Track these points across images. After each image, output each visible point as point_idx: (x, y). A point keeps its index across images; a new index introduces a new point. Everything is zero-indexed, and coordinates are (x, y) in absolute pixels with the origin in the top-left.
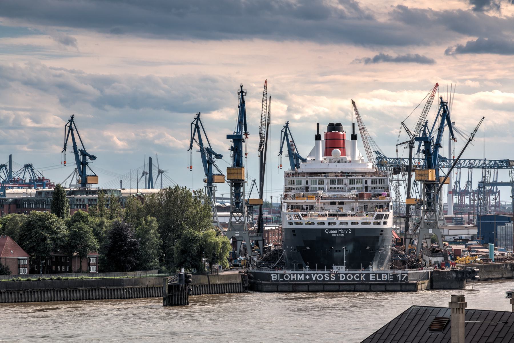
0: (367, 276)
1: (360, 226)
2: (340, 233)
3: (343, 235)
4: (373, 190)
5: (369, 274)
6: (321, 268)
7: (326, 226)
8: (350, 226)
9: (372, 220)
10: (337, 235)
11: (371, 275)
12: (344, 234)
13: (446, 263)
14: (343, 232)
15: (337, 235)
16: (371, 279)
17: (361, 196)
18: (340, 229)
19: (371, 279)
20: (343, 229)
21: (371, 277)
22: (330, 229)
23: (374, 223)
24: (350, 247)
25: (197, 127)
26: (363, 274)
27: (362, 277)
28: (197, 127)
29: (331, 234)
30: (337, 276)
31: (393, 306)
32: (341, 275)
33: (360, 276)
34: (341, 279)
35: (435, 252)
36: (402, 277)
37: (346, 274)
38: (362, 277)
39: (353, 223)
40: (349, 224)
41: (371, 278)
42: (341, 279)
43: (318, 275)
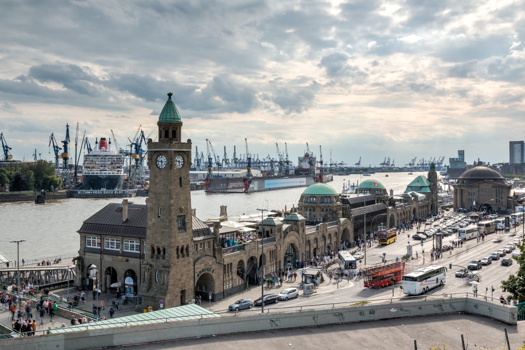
0: (114, 192)
1: (111, 174)
4: (116, 161)
6: (97, 189)
7: (99, 174)
8: (107, 174)
9: (116, 172)
13: (142, 187)
17: (112, 164)
24: (108, 182)
25: (52, 138)
28: (52, 138)
30: (103, 192)
31: (103, 203)
35: (138, 183)
41: (115, 192)
43: (96, 192)
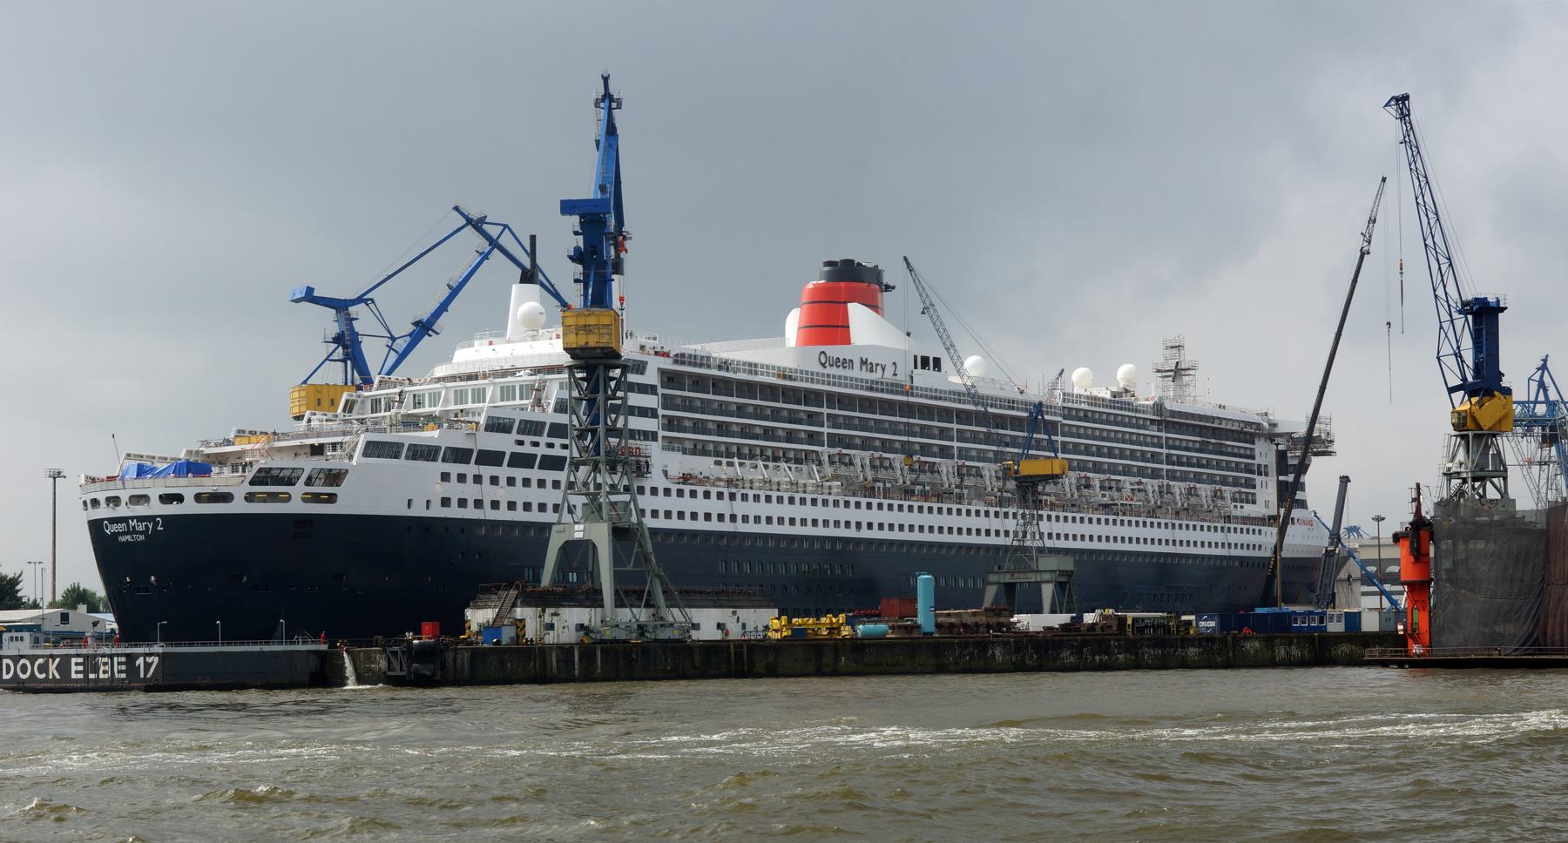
1: (190, 507)
2: (135, 532)
3: (142, 538)
5: (67, 658)
8: (156, 508)
10: (128, 538)
11: (74, 660)
12: (145, 533)
14: (141, 527)
15: (128, 538)
16: (74, 676)
18: (132, 518)
19: (74, 676)
20: (141, 519)
21: (74, 668)
22: (113, 521)
23: (250, 498)
26: (53, 657)
27: (52, 667)
29: (115, 535)
32: (5, 661)
33: (46, 664)
34: (5, 677)
36: (147, 666)
37: (16, 659)
38: (52, 667)
39: (167, 499)
40: (155, 500)
42: (5, 677)
